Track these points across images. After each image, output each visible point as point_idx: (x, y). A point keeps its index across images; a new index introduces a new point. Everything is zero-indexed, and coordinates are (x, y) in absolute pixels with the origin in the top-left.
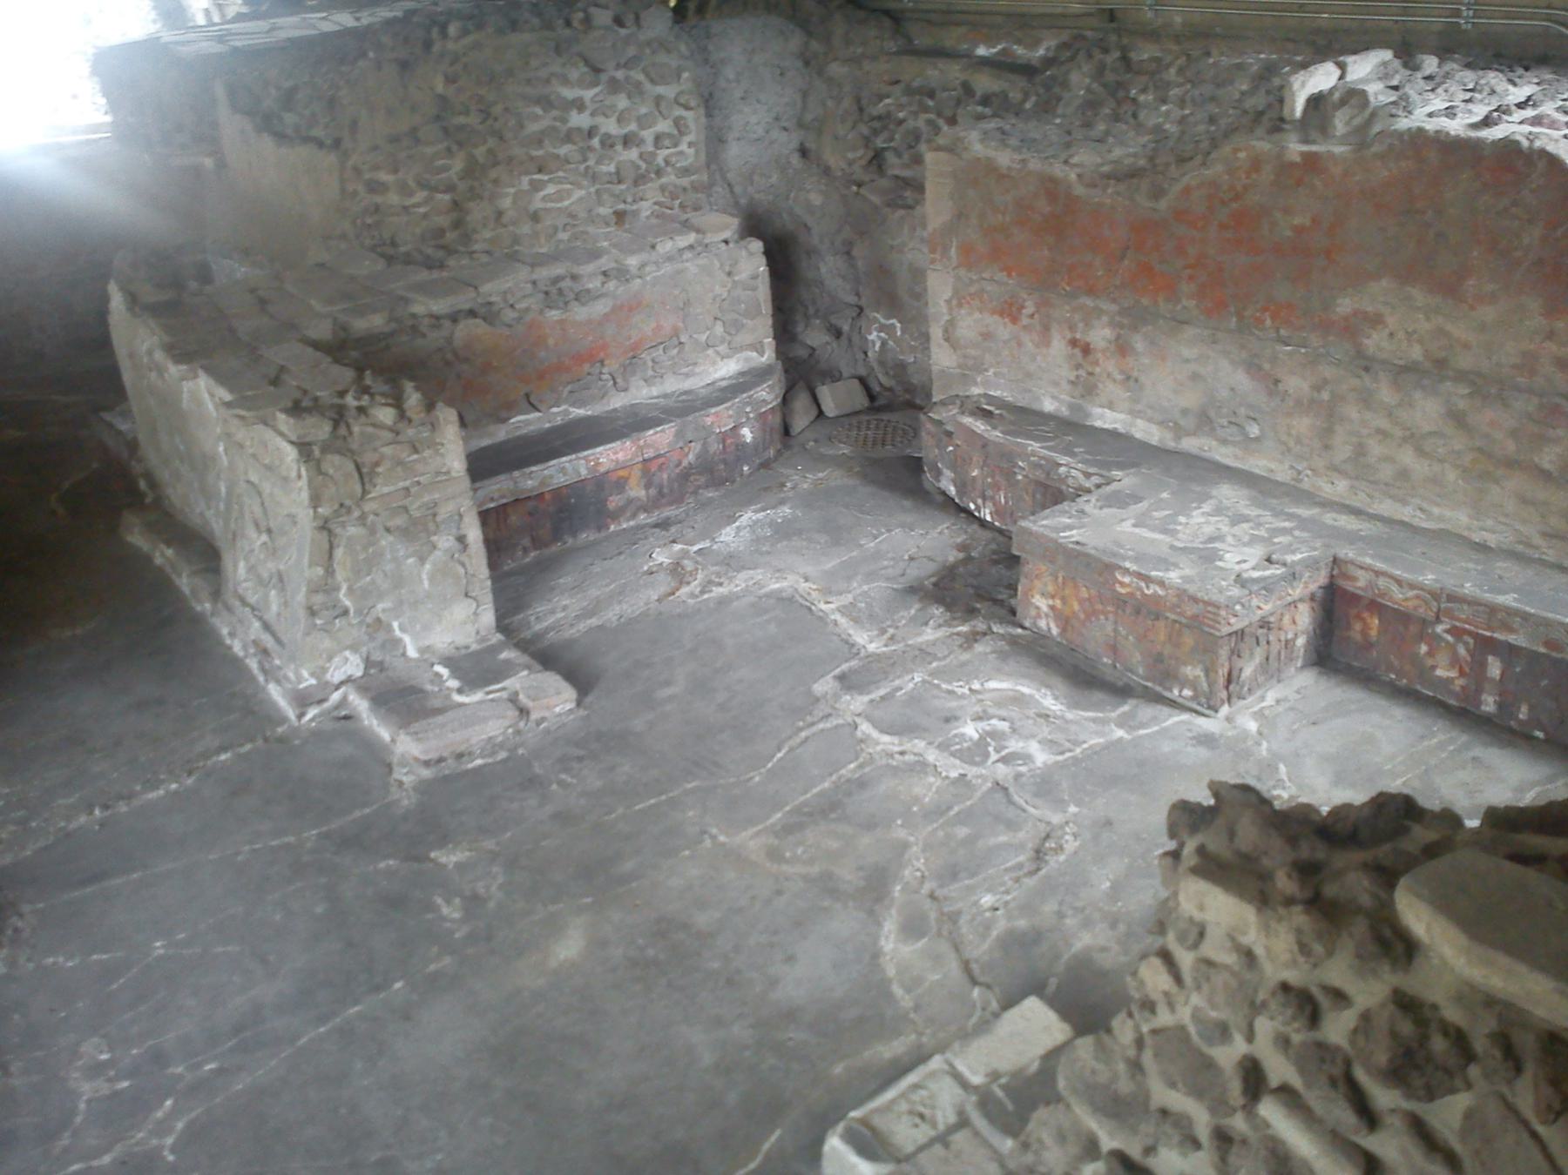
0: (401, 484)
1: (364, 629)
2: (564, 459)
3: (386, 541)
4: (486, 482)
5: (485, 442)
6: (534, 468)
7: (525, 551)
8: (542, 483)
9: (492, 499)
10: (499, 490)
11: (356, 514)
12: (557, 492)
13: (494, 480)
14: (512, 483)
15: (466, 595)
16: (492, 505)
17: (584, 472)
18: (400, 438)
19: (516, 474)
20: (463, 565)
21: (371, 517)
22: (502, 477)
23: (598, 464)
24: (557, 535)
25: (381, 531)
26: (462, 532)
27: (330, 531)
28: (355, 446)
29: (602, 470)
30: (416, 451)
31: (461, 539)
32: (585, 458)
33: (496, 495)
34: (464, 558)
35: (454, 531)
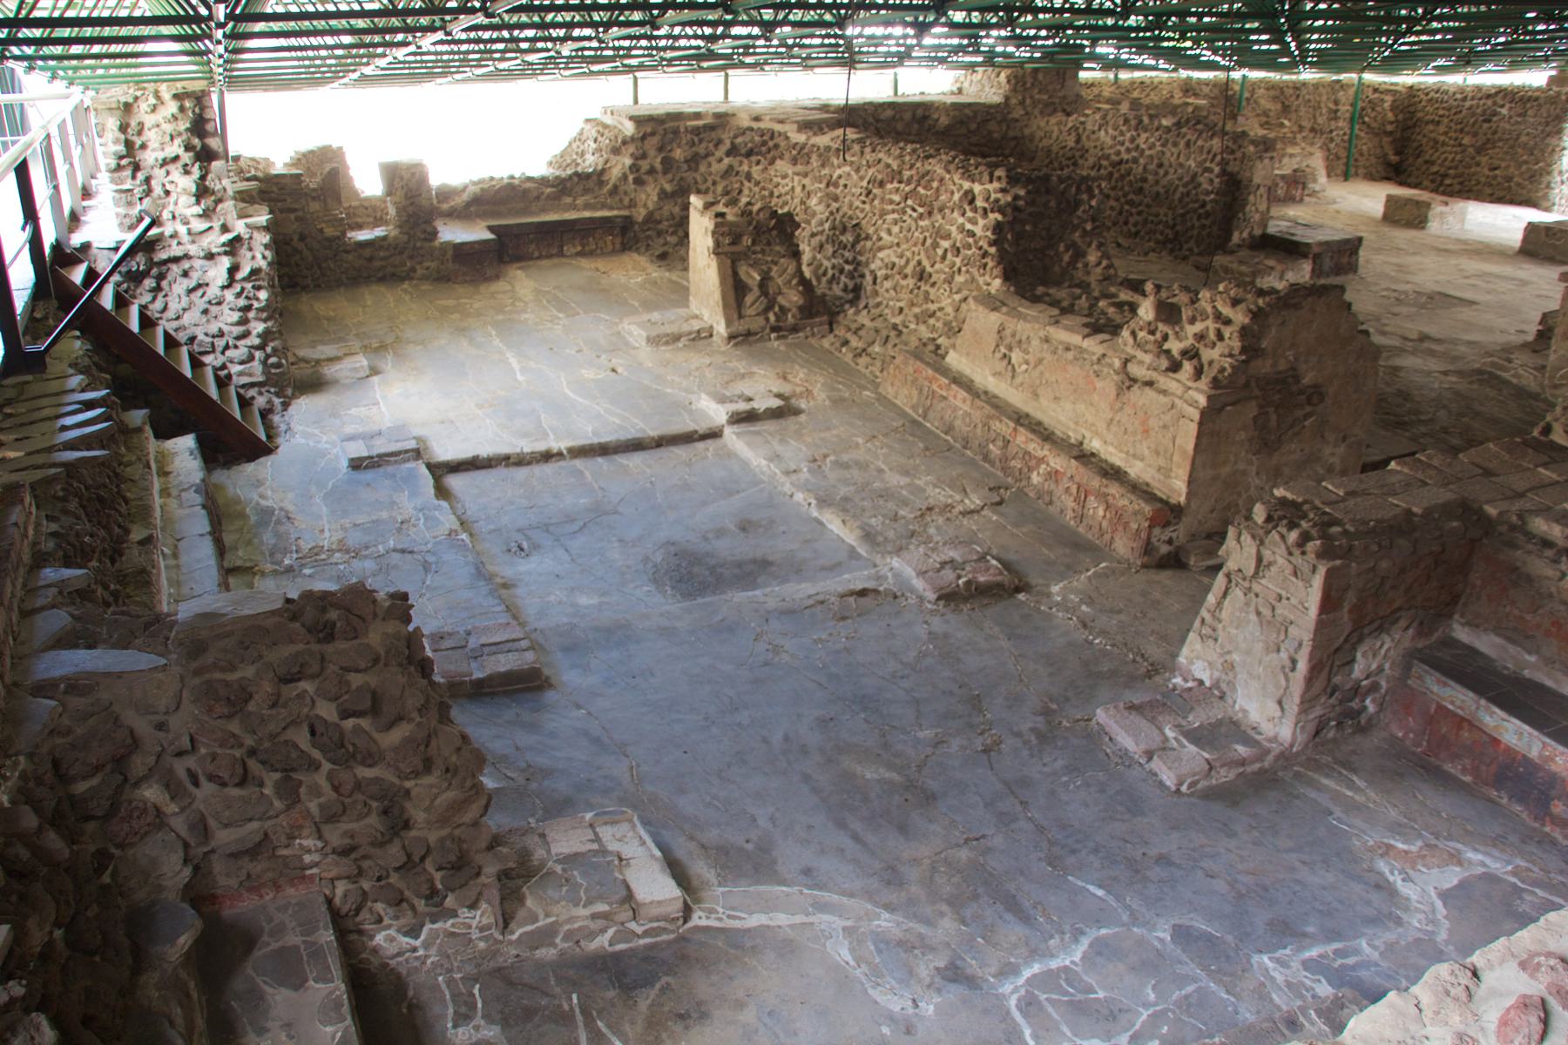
0: (1279, 591)
1: (1222, 660)
2: (1526, 727)
3: (1253, 617)
4: (1458, 687)
5: (1549, 683)
6: (1497, 710)
7: (1464, 771)
8: (1496, 727)
9: (1452, 703)
10: (1463, 701)
11: (1246, 584)
12: (1508, 749)
13: (1464, 690)
14: (1473, 708)
15: (1280, 703)
16: (1450, 707)
17: (1534, 753)
18: (1291, 558)
19: (1483, 702)
20: (1287, 679)
21: (1252, 595)
22: (1471, 694)
23: (1551, 759)
24: (1499, 781)
25: (1252, 608)
26: (1297, 657)
27: (1230, 581)
28: (1267, 541)
29: (1553, 767)
30: (1295, 574)
31: (1294, 662)
32: (1544, 744)
33: (1458, 703)
34: (1291, 674)
35: (1292, 651)
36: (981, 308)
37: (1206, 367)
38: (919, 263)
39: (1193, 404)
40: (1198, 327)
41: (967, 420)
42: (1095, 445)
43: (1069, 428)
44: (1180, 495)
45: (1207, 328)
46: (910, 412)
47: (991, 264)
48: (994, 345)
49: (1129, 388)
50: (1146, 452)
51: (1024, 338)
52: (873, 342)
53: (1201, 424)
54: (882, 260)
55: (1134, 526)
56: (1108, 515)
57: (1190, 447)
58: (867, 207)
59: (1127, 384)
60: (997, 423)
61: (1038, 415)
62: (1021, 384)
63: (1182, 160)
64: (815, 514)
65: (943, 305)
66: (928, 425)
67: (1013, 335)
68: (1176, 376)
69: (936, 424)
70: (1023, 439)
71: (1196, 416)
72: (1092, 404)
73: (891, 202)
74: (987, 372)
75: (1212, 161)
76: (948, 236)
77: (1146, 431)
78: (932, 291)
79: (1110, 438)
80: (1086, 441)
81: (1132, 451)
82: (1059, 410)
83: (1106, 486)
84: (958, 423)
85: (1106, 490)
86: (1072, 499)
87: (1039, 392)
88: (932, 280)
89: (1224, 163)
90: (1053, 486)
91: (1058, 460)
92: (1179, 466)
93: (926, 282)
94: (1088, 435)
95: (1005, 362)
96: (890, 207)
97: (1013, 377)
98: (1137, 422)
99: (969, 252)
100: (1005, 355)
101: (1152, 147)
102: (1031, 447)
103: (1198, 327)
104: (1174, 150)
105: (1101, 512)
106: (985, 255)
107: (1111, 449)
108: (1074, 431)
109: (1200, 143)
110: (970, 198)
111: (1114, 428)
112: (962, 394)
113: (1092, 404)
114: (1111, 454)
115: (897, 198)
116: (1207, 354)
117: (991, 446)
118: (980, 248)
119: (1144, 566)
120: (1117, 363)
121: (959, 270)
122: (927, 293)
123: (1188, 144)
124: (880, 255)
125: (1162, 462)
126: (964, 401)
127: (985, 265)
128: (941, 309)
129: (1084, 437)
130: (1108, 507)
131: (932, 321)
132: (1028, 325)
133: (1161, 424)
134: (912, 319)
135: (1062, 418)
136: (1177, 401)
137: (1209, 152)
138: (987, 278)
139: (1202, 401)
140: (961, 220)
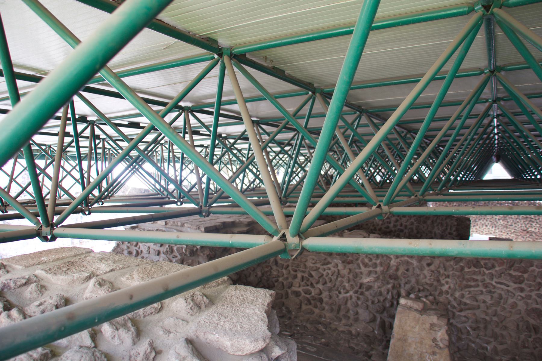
54: (465, 316)
58: (435, 283)
73: (477, 280)
75: (451, 229)
89: (457, 230)
96: (473, 284)
101: (412, 224)
104: (425, 225)
115: (479, 277)
123: (433, 222)
124: (463, 314)
137: (447, 226)
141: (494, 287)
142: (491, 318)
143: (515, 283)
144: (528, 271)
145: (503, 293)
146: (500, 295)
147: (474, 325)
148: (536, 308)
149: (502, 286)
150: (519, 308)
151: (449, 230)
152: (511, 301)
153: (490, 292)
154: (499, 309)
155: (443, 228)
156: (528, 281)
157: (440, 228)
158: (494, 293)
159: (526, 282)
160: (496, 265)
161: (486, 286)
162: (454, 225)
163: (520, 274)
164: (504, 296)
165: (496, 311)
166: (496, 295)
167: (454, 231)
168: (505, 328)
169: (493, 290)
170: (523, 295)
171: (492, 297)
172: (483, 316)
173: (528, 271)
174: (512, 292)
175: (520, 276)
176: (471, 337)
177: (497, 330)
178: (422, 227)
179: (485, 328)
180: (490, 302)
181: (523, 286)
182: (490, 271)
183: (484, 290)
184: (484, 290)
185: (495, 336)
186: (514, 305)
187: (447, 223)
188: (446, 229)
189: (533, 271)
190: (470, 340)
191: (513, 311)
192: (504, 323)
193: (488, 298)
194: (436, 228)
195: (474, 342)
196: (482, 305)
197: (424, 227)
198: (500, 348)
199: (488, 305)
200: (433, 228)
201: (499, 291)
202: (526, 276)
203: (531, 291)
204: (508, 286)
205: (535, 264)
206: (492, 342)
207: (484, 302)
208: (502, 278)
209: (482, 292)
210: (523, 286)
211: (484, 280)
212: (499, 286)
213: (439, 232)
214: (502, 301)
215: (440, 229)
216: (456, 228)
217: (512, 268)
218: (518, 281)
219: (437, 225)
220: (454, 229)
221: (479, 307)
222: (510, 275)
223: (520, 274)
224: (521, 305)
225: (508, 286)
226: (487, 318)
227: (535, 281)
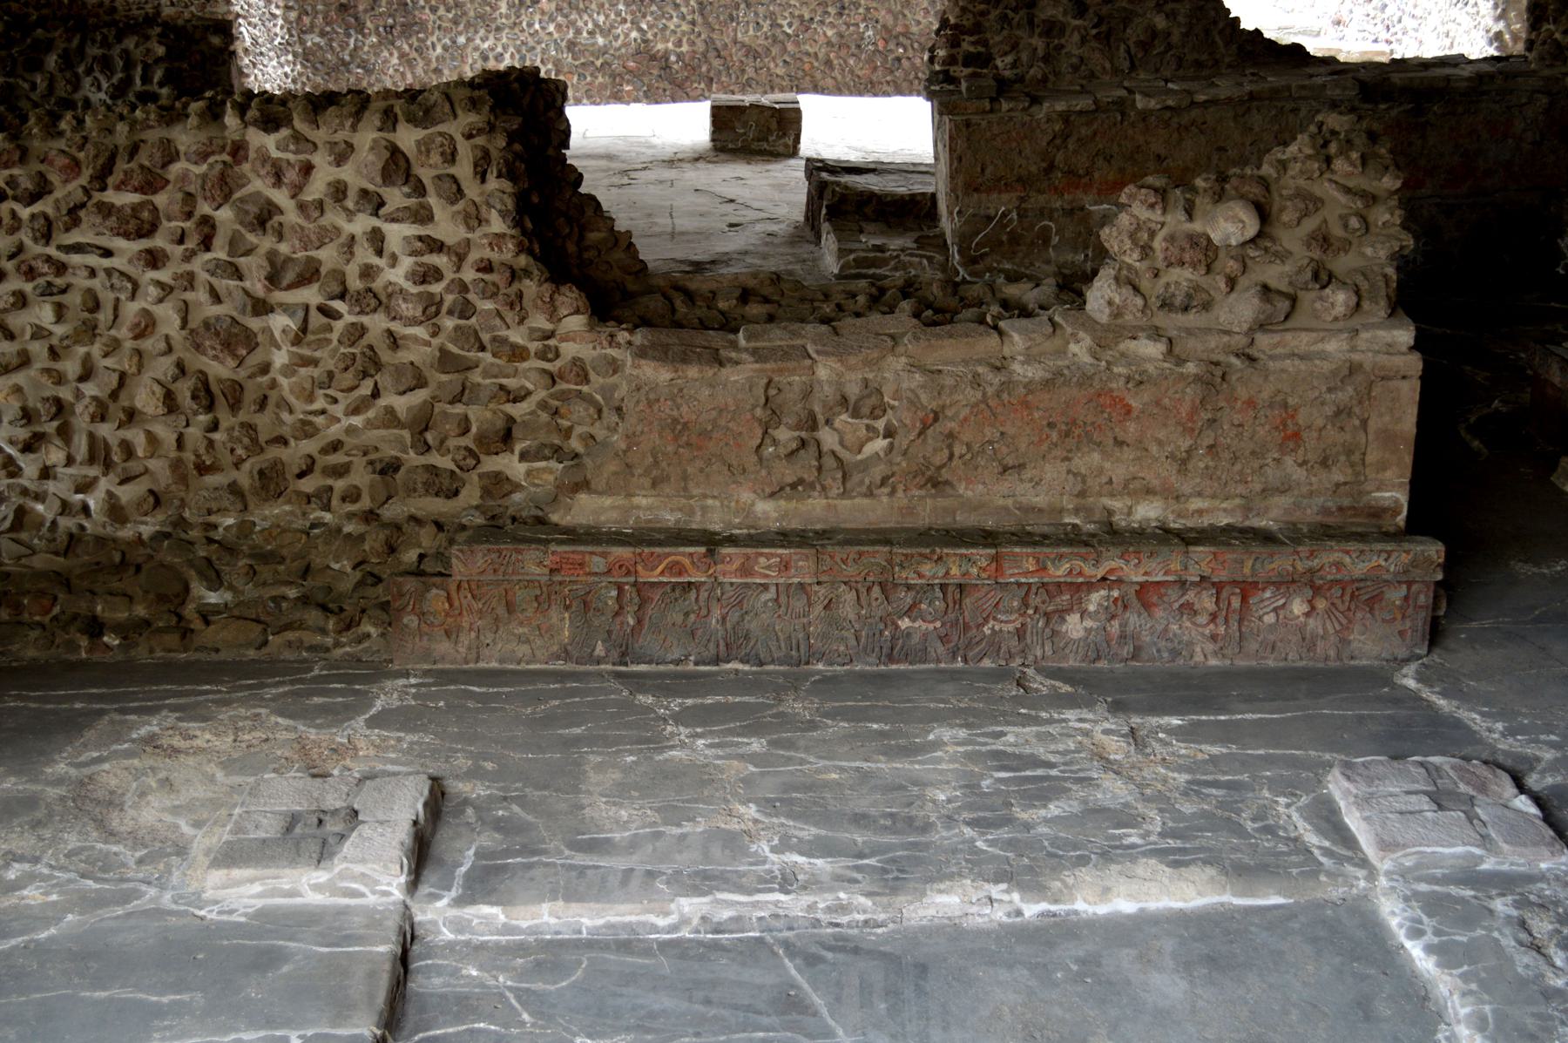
36: (693, 372)
37: (1364, 286)
38: (181, 368)
39: (1390, 349)
40: (1310, 224)
41: (799, 604)
42: (1148, 512)
43: (1061, 511)
44: (1397, 512)
45: (1325, 221)
46: (559, 665)
47: (530, 287)
48: (759, 432)
49: (1223, 378)
50: (1299, 474)
51: (853, 391)
52: (187, 589)
53: (1424, 378)
55: (1396, 595)
56: (1321, 604)
57: (1408, 423)
59: (1218, 372)
60: (927, 569)
61: (964, 519)
62: (884, 482)
63: (62, 89)
64: (1032, 910)
65: (335, 431)
66: (643, 668)
67: (807, 393)
68: (1288, 325)
69: (676, 654)
70: (1030, 565)
71: (1415, 363)
72: (1119, 443)
74: (746, 496)
75: (146, 79)
76: (309, 274)
77: (1296, 436)
78: (263, 421)
79: (1187, 488)
80: (1116, 518)
81: (1258, 487)
82: (1020, 488)
83: (1312, 554)
84: (753, 625)
85: (1316, 563)
86: (1203, 619)
87: (945, 474)
88: (250, 396)
90: (1134, 619)
91: (1152, 565)
92: (1382, 466)
93: (235, 406)
94: (1116, 504)
95: (808, 458)
97: (845, 478)
98: (1261, 432)
99: (436, 288)
100: (803, 443)
102: (1059, 572)
103: (1310, 224)
105: (1298, 607)
106: (514, 275)
107: (1196, 504)
108: (1076, 511)
109: (94, 51)
110: (396, 166)
111: (1200, 462)
112: (766, 562)
113: (1119, 443)
114: (1200, 512)
116: (1342, 263)
117: (905, 623)
118: (486, 267)
119: (1429, 652)
120: (1151, 349)
121: (394, 341)
122: (249, 427)
125: (1337, 476)
126: (785, 566)
127: (520, 295)
128: (335, 446)
129: (1110, 513)
130: (1317, 590)
131: (308, 485)
132: (852, 360)
133: (1329, 410)
134: (227, 500)
135: (1040, 500)
136: (1356, 357)
138: (540, 321)
139: (1404, 335)
140: (362, 224)
141: (61, 268)
142: (79, 395)
143: (127, 236)
144: (168, 182)
145: (96, 284)
146: (91, 294)
147: (23, 434)
148: (218, 318)
149: (93, 260)
150: (163, 329)
151: (138, 81)
152: (131, 309)
153: (48, 291)
154: (96, 350)
155: (115, 80)
156: (169, 220)
157: (102, 78)
158: (63, 291)
159: (165, 223)
160: (54, 178)
161: (31, 274)
162: (158, 60)
163: (135, 198)
164: (107, 297)
165: (87, 360)
166: (74, 299)
167: (161, 85)
168: (131, 416)
169: (59, 281)
170: (164, 275)
171: (60, 312)
172: (50, 390)
173: (168, 182)
174: (122, 273)
175: (136, 209)
176: (24, 482)
177: (105, 430)
178: (26, 86)
179: (65, 433)
180: (59, 330)
181: (159, 241)
182: (37, 208)
183: (28, 287)
184: (28, 287)
185: (99, 454)
186: (145, 328)
187: (126, 52)
188: (127, 82)
189: (184, 177)
190: (25, 492)
191: (147, 344)
192: (124, 401)
193: (44, 314)
194: (87, 81)
195: (40, 497)
196: (38, 349)
197: (34, 86)
198: (126, 494)
199: (55, 341)
200: (77, 86)
201: (81, 281)
202: (160, 199)
203: (189, 257)
204: (107, 253)
205: (182, 149)
206: (95, 479)
207: (39, 333)
208: (84, 226)
209: (21, 301)
210: (159, 241)
211: (20, 249)
212: (76, 259)
213: (102, 96)
214: (104, 316)
215: (105, 85)
216: (167, 70)
217: (111, 181)
218: (131, 227)
219: (89, 72)
220: (158, 74)
221: (25, 360)
222: (106, 210)
223: (135, 198)
224: (168, 315)
225: (107, 253)
226: (65, 394)
227: (189, 215)
